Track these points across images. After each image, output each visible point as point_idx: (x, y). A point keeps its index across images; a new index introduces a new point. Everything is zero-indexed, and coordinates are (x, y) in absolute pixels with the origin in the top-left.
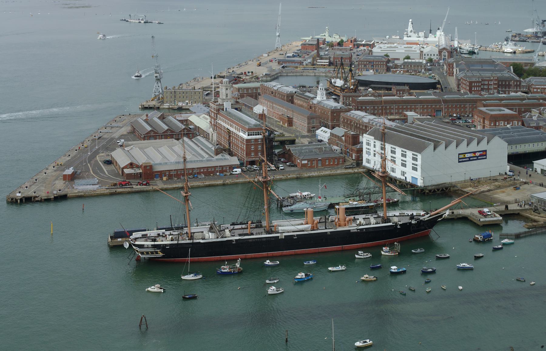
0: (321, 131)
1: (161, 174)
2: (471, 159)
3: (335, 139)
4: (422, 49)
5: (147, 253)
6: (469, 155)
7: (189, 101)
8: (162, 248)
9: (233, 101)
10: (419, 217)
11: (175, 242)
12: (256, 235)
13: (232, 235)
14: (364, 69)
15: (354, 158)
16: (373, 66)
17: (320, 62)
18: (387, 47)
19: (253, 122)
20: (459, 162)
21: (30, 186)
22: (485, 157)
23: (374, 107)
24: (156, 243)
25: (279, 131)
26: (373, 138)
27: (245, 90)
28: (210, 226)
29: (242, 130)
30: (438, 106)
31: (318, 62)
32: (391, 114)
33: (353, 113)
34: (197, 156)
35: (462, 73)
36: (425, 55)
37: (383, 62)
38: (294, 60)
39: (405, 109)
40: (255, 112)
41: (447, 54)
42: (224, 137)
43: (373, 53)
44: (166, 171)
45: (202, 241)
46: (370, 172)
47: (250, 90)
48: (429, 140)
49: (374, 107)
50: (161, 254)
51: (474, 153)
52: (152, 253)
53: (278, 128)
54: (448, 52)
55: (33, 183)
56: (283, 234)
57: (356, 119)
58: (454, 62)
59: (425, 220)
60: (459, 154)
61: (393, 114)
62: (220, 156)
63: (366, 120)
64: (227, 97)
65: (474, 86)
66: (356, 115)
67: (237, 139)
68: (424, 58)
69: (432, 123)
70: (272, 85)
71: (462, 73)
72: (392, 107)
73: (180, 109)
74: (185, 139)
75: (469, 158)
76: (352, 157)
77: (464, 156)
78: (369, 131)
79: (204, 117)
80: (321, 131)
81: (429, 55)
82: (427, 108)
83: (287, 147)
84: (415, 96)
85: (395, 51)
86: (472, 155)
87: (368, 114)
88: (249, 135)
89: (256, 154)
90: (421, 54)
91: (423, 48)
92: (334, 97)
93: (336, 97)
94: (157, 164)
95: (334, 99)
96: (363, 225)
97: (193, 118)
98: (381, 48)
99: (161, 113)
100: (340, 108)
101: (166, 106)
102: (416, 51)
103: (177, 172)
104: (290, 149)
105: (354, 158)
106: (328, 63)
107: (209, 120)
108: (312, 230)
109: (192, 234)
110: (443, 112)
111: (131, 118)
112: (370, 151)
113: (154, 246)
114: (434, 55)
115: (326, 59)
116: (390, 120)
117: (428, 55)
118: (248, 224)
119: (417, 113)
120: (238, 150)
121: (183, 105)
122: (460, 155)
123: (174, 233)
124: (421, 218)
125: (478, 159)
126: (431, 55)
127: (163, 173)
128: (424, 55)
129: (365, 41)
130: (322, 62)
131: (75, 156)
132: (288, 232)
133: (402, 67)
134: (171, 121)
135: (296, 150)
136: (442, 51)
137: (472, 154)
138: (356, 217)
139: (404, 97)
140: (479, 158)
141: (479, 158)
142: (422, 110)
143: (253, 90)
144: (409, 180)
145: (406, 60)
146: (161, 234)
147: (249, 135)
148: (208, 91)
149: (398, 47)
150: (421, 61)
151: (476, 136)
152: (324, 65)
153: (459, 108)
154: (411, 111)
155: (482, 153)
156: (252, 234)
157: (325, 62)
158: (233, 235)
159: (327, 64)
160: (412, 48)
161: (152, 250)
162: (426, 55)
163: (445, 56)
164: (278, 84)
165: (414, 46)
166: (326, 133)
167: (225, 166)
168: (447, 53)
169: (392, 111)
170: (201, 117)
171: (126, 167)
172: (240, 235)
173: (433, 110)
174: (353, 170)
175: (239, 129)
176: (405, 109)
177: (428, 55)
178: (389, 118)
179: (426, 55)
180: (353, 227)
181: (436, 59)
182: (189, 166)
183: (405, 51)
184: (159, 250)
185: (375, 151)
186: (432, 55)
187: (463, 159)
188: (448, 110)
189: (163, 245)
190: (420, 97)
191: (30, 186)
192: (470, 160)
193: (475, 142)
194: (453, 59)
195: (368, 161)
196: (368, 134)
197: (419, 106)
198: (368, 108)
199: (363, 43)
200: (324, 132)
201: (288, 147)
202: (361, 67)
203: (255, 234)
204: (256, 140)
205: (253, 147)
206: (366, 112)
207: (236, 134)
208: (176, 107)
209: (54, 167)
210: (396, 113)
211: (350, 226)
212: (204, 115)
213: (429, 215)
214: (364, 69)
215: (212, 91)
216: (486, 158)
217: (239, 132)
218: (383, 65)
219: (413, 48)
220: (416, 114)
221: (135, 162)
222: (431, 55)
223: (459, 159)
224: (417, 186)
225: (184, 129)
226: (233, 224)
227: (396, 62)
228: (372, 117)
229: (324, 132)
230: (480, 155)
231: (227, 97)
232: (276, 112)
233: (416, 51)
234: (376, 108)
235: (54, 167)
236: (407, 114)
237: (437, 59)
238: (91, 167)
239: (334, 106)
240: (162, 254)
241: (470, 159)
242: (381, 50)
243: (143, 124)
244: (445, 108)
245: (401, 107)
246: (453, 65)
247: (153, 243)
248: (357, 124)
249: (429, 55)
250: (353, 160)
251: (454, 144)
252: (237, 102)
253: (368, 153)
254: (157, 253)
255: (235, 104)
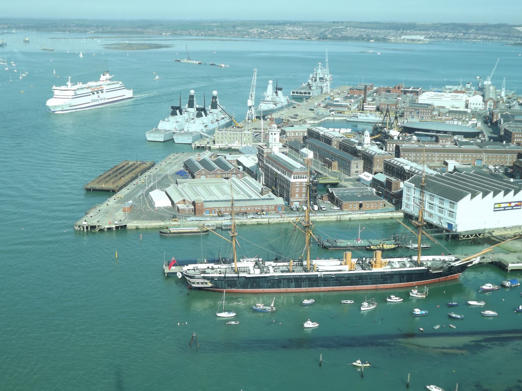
0: (364, 175)
1: (211, 210)
2: (506, 208)
3: (377, 184)
4: (468, 98)
5: (198, 283)
6: (504, 205)
7: (239, 142)
8: (211, 279)
9: (281, 145)
10: (450, 263)
11: (223, 275)
12: (297, 272)
13: (275, 272)
14: (409, 115)
15: (394, 202)
16: (418, 113)
17: (367, 108)
18: (434, 95)
19: (298, 165)
20: (495, 211)
21: (95, 216)
22: (520, 207)
23: (416, 154)
24: (206, 275)
25: (323, 174)
26: (414, 185)
27: (293, 133)
28: (255, 263)
29: (287, 173)
30: (478, 156)
31: (365, 108)
32: (433, 161)
33: (395, 161)
34: (245, 195)
35: (506, 124)
36: (470, 104)
37: (428, 110)
38: (342, 105)
39: (446, 157)
40: (301, 154)
41: (492, 104)
42: (271, 178)
43: (419, 101)
44: (215, 208)
45: (246, 275)
46: (408, 217)
47: (297, 133)
48: (466, 189)
49: (416, 154)
50: (210, 285)
51: (510, 203)
52: (202, 283)
53: (322, 171)
54: (494, 102)
55: (96, 213)
56: (323, 272)
57: (398, 166)
58: (499, 112)
59: (456, 265)
60: (495, 204)
61: (435, 161)
62: (266, 196)
63: (407, 168)
64: (275, 141)
65: (517, 138)
66: (398, 162)
67: (283, 181)
68: (469, 107)
69: (471, 173)
70: (319, 130)
71: (506, 124)
72: (434, 155)
73: (230, 150)
74: (234, 178)
75: (505, 207)
76: (392, 202)
77: (500, 205)
78: (410, 178)
79: (253, 159)
80: (364, 175)
81: (475, 104)
82: (468, 157)
83: (330, 190)
84: (457, 145)
85: (441, 99)
86: (508, 205)
87: (410, 162)
88: (294, 178)
89: (301, 196)
90: (466, 103)
91: (469, 96)
92: (378, 143)
93: (380, 143)
94: (207, 202)
95: (378, 145)
96: (398, 268)
97: (242, 159)
98: (427, 95)
99: (213, 153)
100: (384, 155)
101: (217, 146)
102: (462, 100)
103: (226, 209)
104: (332, 192)
105: (394, 202)
106: (374, 109)
107: (257, 161)
108: (349, 271)
109: (238, 269)
110: (483, 162)
111: (184, 156)
112: (409, 197)
113: (204, 278)
114: (480, 104)
115: (373, 105)
116: (430, 168)
117: (474, 104)
118: (290, 262)
119: (458, 161)
120: (284, 192)
121: (233, 145)
122: (496, 205)
123: (222, 267)
124: (453, 264)
125: (512, 209)
126: (477, 104)
127: (213, 210)
128: (469, 104)
129: (412, 88)
130: (369, 108)
131: (133, 191)
132: (327, 271)
133: (447, 115)
134: (221, 161)
135: (338, 193)
136: (488, 101)
137: (508, 204)
138: (391, 260)
139: (446, 146)
140: (514, 208)
141: (514, 208)
142: (462, 159)
143: (300, 133)
144: (446, 226)
145: (451, 109)
146: (210, 267)
147: (294, 178)
148: (258, 132)
149: (444, 95)
150: (466, 110)
151: (513, 188)
152: (371, 111)
153: (499, 158)
154: (452, 159)
155: (517, 203)
156: (293, 271)
157: (371, 108)
158: (276, 271)
159: (373, 110)
160: (458, 96)
161: (202, 281)
162: (472, 104)
163: (490, 106)
164: (325, 128)
165: (461, 95)
166: (368, 177)
167: (271, 205)
168: (492, 102)
169: (434, 158)
170: (250, 158)
171: (179, 203)
172: (282, 272)
173: (474, 160)
174: (392, 213)
175: (285, 172)
176: (446, 157)
177: (474, 104)
178: (430, 165)
179: (472, 104)
180: (387, 269)
181: (481, 108)
182: (236, 204)
183: (451, 99)
184: (208, 281)
185: (414, 197)
186: (478, 104)
187: (497, 208)
188: (488, 159)
189: (212, 277)
190: (462, 147)
191: (95, 216)
192: (504, 210)
193: (512, 192)
194: (499, 109)
195: (407, 205)
196: (408, 182)
197: (461, 155)
198: (410, 155)
199: (411, 89)
200: (366, 176)
201: (331, 190)
202: (407, 114)
203: (296, 272)
204: (301, 183)
205: (297, 189)
206: (408, 160)
207: (282, 177)
208: (227, 147)
209: (115, 199)
210: (437, 161)
211: (385, 268)
212: (252, 156)
213: (460, 261)
214: (409, 115)
215: (261, 133)
216: (520, 208)
217: (285, 175)
218: (428, 112)
219: (459, 97)
220: (457, 163)
221: (187, 198)
222: (477, 104)
223: (495, 208)
224: (453, 232)
225: (233, 169)
226: (276, 260)
227: (442, 110)
228: (414, 165)
229: (366, 176)
230: (516, 205)
231: (275, 141)
232: (322, 156)
233: (462, 100)
234: (418, 155)
235: (115, 199)
236: (448, 162)
237: (482, 108)
238: (148, 201)
239: (378, 152)
240: (211, 285)
241: (505, 209)
242: (428, 98)
243: (195, 163)
244: (486, 158)
245: (442, 155)
246: (497, 115)
247: (202, 275)
248: (399, 170)
249: (475, 104)
250: (393, 204)
251: (492, 194)
252: (284, 146)
253: (408, 199)
254: (206, 283)
255: (282, 148)
